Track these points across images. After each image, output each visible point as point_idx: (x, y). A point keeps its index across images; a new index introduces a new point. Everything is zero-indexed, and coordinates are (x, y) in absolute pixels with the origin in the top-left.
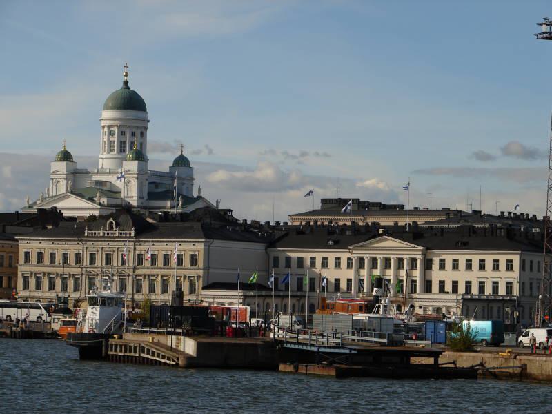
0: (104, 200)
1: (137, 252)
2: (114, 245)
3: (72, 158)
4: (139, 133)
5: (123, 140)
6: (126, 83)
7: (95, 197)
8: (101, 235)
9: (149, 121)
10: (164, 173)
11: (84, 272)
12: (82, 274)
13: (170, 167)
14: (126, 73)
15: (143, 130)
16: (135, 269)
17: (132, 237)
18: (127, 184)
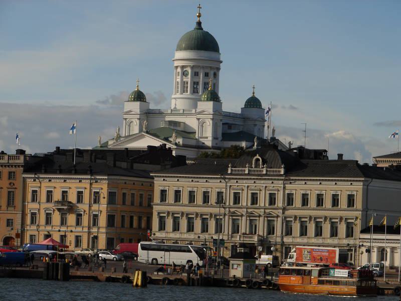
0: (180, 141)
1: (287, 192)
2: (261, 184)
3: (145, 99)
4: (211, 73)
5: (196, 80)
6: (199, 23)
7: (171, 137)
8: (247, 172)
9: (221, 62)
10: (237, 114)
11: (227, 213)
12: (225, 215)
13: (242, 108)
14: (200, 14)
15: (215, 71)
16: (284, 209)
17: (281, 175)
18: (202, 124)
